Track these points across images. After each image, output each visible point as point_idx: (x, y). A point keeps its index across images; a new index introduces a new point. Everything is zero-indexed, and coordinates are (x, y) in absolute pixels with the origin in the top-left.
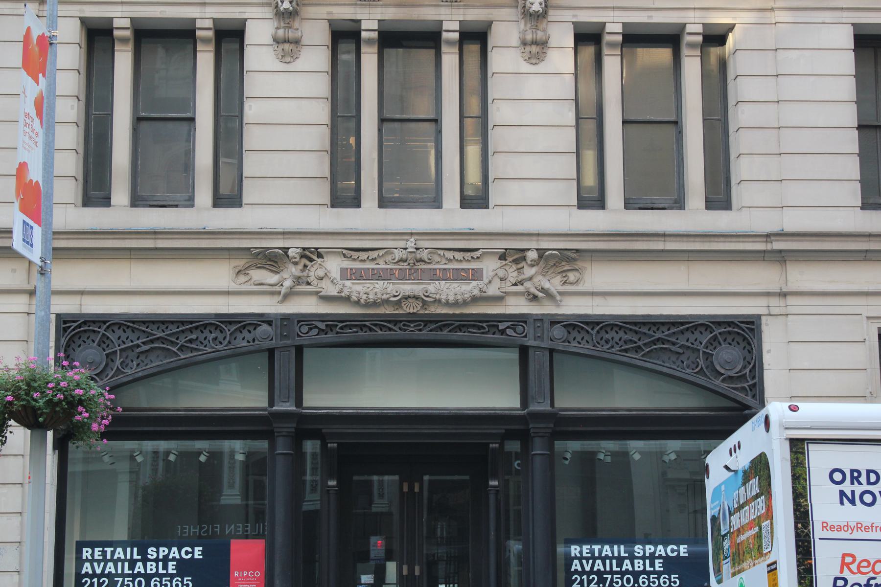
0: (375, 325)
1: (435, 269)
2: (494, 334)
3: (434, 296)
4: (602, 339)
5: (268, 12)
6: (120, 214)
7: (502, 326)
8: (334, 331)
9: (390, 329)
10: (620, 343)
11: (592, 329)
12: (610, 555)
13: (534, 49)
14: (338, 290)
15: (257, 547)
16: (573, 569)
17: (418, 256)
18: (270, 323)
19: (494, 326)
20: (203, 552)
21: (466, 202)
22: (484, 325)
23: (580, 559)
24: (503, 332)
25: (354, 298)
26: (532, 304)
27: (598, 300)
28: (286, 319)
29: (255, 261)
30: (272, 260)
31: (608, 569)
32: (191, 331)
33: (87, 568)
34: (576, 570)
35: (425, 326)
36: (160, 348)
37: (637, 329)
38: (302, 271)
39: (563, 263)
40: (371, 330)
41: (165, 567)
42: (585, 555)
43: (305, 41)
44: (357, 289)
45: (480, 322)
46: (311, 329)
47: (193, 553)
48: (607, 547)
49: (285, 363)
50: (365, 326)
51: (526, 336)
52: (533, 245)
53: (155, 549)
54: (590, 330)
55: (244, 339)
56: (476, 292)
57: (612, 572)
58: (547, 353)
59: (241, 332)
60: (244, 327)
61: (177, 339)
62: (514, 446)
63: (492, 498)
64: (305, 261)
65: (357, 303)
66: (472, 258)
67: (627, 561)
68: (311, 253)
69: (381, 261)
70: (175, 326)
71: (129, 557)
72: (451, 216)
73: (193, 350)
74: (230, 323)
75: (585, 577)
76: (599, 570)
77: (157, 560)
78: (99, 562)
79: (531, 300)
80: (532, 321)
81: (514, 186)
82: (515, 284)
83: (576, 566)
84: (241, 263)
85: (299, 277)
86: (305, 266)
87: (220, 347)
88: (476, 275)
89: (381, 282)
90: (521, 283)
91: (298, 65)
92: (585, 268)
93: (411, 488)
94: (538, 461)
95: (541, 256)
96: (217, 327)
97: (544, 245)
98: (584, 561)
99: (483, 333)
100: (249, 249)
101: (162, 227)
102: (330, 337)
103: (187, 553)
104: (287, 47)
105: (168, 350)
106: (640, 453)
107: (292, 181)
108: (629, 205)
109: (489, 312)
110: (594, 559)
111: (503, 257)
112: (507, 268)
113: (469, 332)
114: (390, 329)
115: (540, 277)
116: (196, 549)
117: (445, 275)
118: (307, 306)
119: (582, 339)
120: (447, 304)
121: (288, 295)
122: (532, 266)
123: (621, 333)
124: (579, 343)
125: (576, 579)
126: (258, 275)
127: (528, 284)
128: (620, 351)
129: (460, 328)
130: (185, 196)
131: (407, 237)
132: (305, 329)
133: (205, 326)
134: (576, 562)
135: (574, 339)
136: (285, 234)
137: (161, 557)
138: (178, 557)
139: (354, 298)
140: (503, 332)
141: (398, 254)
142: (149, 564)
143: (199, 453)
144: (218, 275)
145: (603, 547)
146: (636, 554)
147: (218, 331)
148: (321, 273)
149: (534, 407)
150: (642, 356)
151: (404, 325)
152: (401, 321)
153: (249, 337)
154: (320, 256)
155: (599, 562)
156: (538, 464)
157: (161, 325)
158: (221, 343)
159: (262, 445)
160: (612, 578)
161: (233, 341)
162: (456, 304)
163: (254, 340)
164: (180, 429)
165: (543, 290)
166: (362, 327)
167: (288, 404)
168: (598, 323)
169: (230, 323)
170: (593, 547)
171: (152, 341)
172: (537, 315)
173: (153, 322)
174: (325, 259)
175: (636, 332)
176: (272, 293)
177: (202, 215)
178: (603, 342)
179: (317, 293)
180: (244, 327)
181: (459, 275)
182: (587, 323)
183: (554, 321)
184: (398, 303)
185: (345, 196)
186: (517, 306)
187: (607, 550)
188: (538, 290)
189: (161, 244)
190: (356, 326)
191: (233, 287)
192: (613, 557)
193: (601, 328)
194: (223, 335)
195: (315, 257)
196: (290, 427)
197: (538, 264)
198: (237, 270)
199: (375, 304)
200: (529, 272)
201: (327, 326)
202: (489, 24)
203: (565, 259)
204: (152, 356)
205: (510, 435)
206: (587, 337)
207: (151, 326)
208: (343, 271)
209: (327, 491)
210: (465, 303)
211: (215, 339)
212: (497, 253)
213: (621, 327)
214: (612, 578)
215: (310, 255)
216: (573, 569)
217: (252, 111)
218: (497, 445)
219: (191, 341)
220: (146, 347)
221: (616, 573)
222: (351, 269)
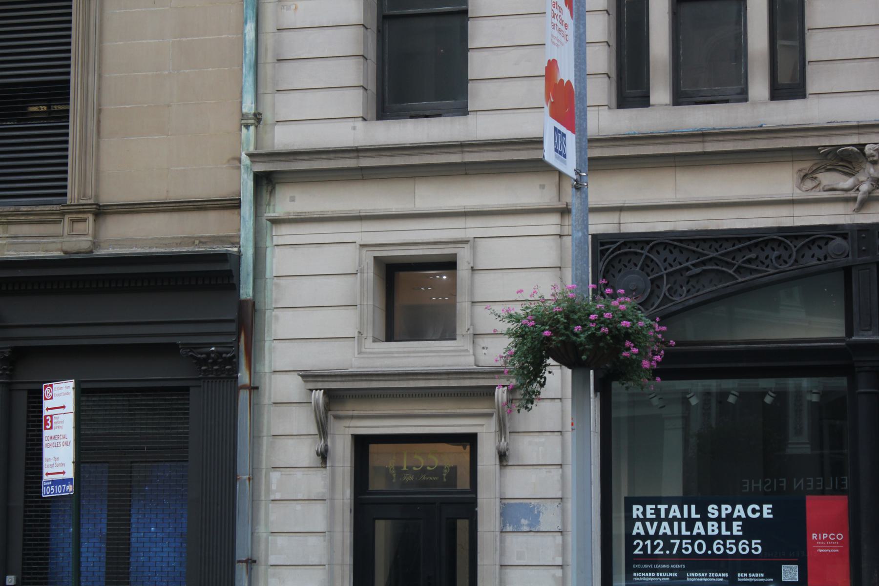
6: (661, 114)
15: (838, 505)
18: (844, 236)
20: (773, 511)
30: (846, 160)
32: (749, 248)
33: (638, 528)
41: (729, 528)
47: (761, 511)
53: (716, 507)
55: (813, 256)
59: (810, 248)
60: (813, 242)
71: (686, 516)
73: (752, 271)
74: (796, 237)
77: (719, 520)
78: (652, 521)
84: (807, 165)
87: (784, 267)
96: (780, 243)
100: (816, 148)
103: (754, 511)
105: (723, 272)
116: (765, 507)
121: (865, 203)
126: (828, 179)
133: (766, 242)
136: (861, 128)
137: (723, 516)
138: (743, 516)
143: (764, 394)
144: (780, 182)
158: (786, 262)
159: (840, 383)
163: (826, 258)
164: (740, 365)
167: (870, 333)
169: (796, 237)
171: (704, 263)
173: (705, 240)
176: (846, 200)
177: (760, 110)
180: (813, 242)
189: (712, 147)
191: (799, 194)
198: (802, 174)
211: (779, 257)
219: (749, 261)
220: (698, 270)
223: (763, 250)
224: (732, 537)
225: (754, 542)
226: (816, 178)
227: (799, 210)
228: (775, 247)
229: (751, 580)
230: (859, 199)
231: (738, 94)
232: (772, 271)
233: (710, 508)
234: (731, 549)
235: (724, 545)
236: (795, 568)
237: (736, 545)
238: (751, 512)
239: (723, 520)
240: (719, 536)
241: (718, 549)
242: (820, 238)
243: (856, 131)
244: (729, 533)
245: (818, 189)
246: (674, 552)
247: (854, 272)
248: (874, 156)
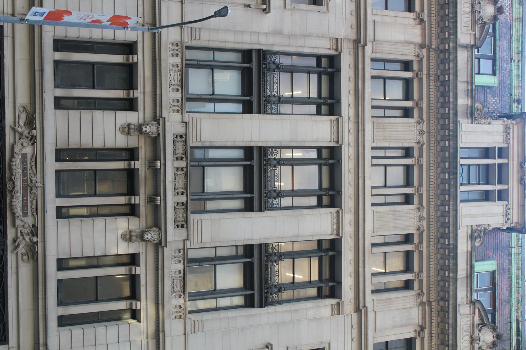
1: (27, 196)
5: (141, 121)
6: (50, 55)
13: (128, 236)
14: (17, 152)
17: (33, 188)
21: (59, 209)
25: (13, 160)
27: (14, 270)
30: (30, 123)
38: (26, 136)
43: (129, 137)
44: (18, 161)
52: (40, 239)
56: (17, 215)
64: (30, 137)
65: (11, 161)
68: (34, 140)
69: (31, 172)
72: (52, 202)
81: (66, 230)
82: (21, 232)
84: (29, 109)
86: (28, 137)
88: (25, 215)
90: (22, 235)
91: (119, 135)
97: (40, 244)
100: (35, 112)
104: (127, 129)
107: (67, 131)
108: (59, 282)
109: (8, 221)
111: (34, 226)
112: (29, 228)
115: (24, 243)
117: (25, 200)
118: (9, 138)
120: (11, 202)
122: (30, 239)
126: (23, 116)
127: (21, 238)
131: (42, 183)
139: (13, 160)
141: (34, 179)
144: (23, 99)
148: (25, 144)
154: (33, 144)
162: (11, 206)
165: (19, 245)
168: (3, 270)
176: (15, 123)
179: (15, 143)
181: (25, 206)
184: (11, 179)
185: (61, 155)
186: (11, 233)
189: (37, 74)
195: (32, 142)
199: (10, 169)
200: (27, 238)
202: (138, 216)
203: (34, 254)
208: (26, 155)
210: (12, 210)
215: (33, 139)
217: (98, 114)
227: (11, 105)
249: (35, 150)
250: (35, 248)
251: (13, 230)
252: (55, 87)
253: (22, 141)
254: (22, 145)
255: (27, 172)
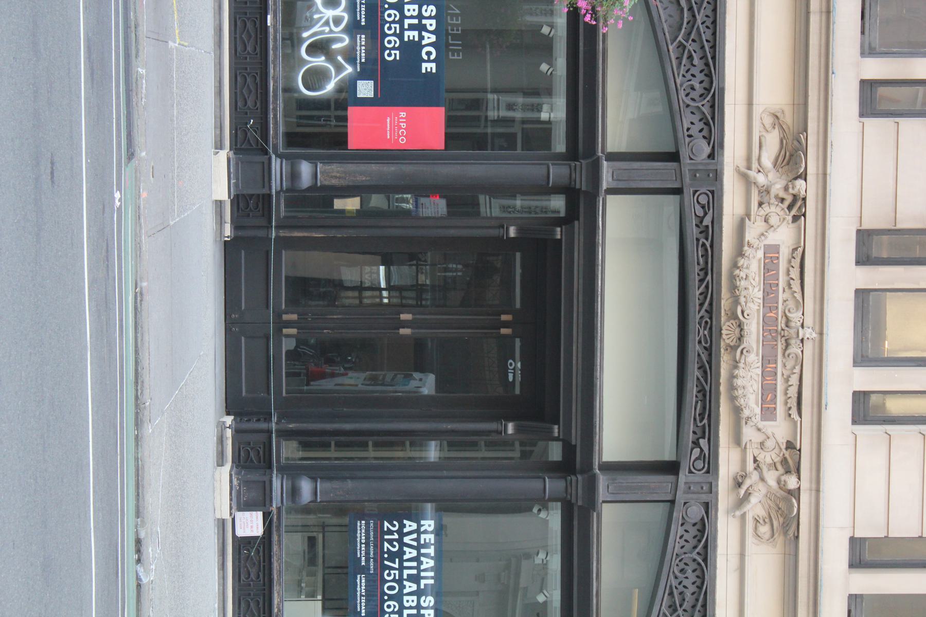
0: (707, 287)
1: (776, 363)
2: (694, 433)
3: (742, 361)
4: (686, 564)
7: (703, 443)
8: (700, 236)
9: (701, 305)
10: (681, 588)
11: (698, 553)
12: (422, 567)
14: (752, 241)
15: (436, 139)
16: (405, 522)
17: (793, 342)
18: (711, 156)
19: (704, 432)
20: (429, 74)
21: (861, 399)
22: (705, 421)
23: (418, 531)
24: (696, 444)
25: (741, 262)
26: (731, 480)
27: (734, 561)
28: (717, 176)
29: (790, 138)
30: (791, 158)
31: (406, 564)
32: (704, 57)
34: (405, 587)
35: (705, 348)
36: (682, 18)
37: (699, 607)
38: (776, 197)
39: (781, 520)
40: (701, 281)
41: (412, 27)
42: (423, 536)
44: (753, 265)
45: (709, 415)
46: (703, 207)
47: (429, 61)
48: (432, 563)
49: (663, 173)
50: (706, 274)
51: (690, 472)
52: (805, 484)
53: (433, 14)
54: (697, 550)
55: (692, 123)
56: (746, 413)
57: (401, 568)
58: (669, 498)
59: (700, 120)
60: (707, 124)
61: (693, 41)
62: (555, 452)
63: (493, 426)
64: (789, 199)
65: (735, 265)
66: (790, 408)
67: (414, 587)
68: (800, 208)
69: (787, 295)
70: (710, 38)
71: (423, 574)
73: (679, 59)
74: (713, 106)
75: (396, 536)
76: (404, 553)
77: (420, 17)
78: (417, 540)
79: (735, 479)
80: (710, 480)
82: (755, 460)
83: (410, 526)
84: (788, 119)
85: (768, 192)
86: (782, 200)
87: (682, 94)
88: (768, 413)
89: (760, 294)
90: (758, 468)
92: (775, 546)
93: (506, 325)
94: (536, 485)
95: (790, 492)
96: (708, 90)
97: (805, 497)
98: (415, 536)
99: (695, 419)
100: (806, 130)
101: (836, 6)
102: (693, 231)
103: (429, 54)
105: (680, 29)
106: (545, 603)
107: (891, 182)
108: (855, 600)
109: (721, 428)
110: (418, 548)
111: (790, 445)
112: (777, 450)
113: (697, 402)
114: (701, 305)
115: (764, 491)
116: (433, 65)
117: (768, 374)
118: (732, 201)
119: (686, 541)
120: (732, 377)
122: (779, 482)
123: (692, 588)
124: (681, 537)
125: (394, 526)
127: (755, 476)
128: (671, 587)
129: (702, 391)
130: (876, 43)
131: (817, 328)
132: (703, 200)
133: (709, 75)
134: (414, 526)
135: (686, 531)
137: (424, 22)
138: (424, 43)
139: (741, 262)
140: (696, 444)
141: (795, 316)
142: (415, 598)
143: (551, 64)
144: (773, 92)
145: (432, 558)
146: (423, 598)
147: (703, 91)
148: (774, 220)
149: (602, 481)
150: (664, 614)
151: (706, 322)
152: (711, 318)
153: (694, 131)
154: (795, 219)
155: (414, 553)
156: (534, 485)
157: (711, 20)
158: (687, 95)
159: (560, 146)
160: (395, 569)
161: (688, 110)
162: (732, 388)
163: (690, 136)
164: (581, 44)
165: (748, 494)
166: (704, 270)
167: (610, 179)
168: (705, 560)
169: (713, 106)
170: (433, 547)
171: (691, 9)
172: (717, 485)
173: (715, 10)
174: (792, 225)
175: (694, 607)
176: (749, 159)
177: (850, 67)
178: (682, 565)
179: (748, 215)
180: (707, 124)
182: (705, 547)
183: (708, 507)
186: (728, 461)
187: (428, 563)
188: (748, 489)
189: (815, 21)
190: (707, 263)
191: (757, 110)
192: (419, 571)
193: (699, 564)
194: (696, 97)
195: (794, 212)
196: (582, 184)
197: (780, 488)
198: (778, 115)
199: (733, 287)
200: (771, 477)
201: (707, 227)
203: (787, 521)
204: (673, 9)
205: (569, 450)
206: (688, 547)
207: (711, 7)
208: (776, 248)
209: (502, 225)
210: (733, 399)
211: (693, 88)
212: (796, 439)
213: (700, 588)
214: (395, 569)
215: (796, 207)
216: (405, 522)
218: (556, 435)
219: (690, 57)
221: (401, 575)
222: (778, 258)
223: (701, 72)
224: (402, 29)
225: (398, 52)
226: (774, 128)
227: (741, 110)
228: (704, 85)
229: (358, 48)
230: (749, 172)
231: (870, 44)
232: (678, 81)
233: (432, 7)
234: (389, 28)
235: (394, 22)
236: (371, 95)
237: (394, 34)
238: (428, 50)
239: (419, 612)
240: (403, 17)
241: (390, 15)
242: (710, 131)
243: (821, 171)
244: (406, 27)
245: (762, 129)
246: (386, 562)
247: (674, 165)
248: (793, 188)
249: (801, 234)
250: (792, 506)
251: (735, 454)
252: (863, 54)
253: (766, 209)
254: (766, 221)
255: (777, 297)
